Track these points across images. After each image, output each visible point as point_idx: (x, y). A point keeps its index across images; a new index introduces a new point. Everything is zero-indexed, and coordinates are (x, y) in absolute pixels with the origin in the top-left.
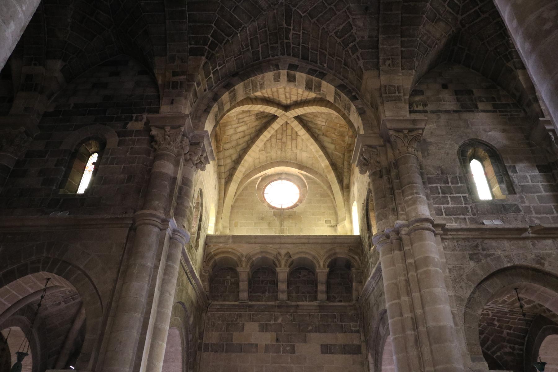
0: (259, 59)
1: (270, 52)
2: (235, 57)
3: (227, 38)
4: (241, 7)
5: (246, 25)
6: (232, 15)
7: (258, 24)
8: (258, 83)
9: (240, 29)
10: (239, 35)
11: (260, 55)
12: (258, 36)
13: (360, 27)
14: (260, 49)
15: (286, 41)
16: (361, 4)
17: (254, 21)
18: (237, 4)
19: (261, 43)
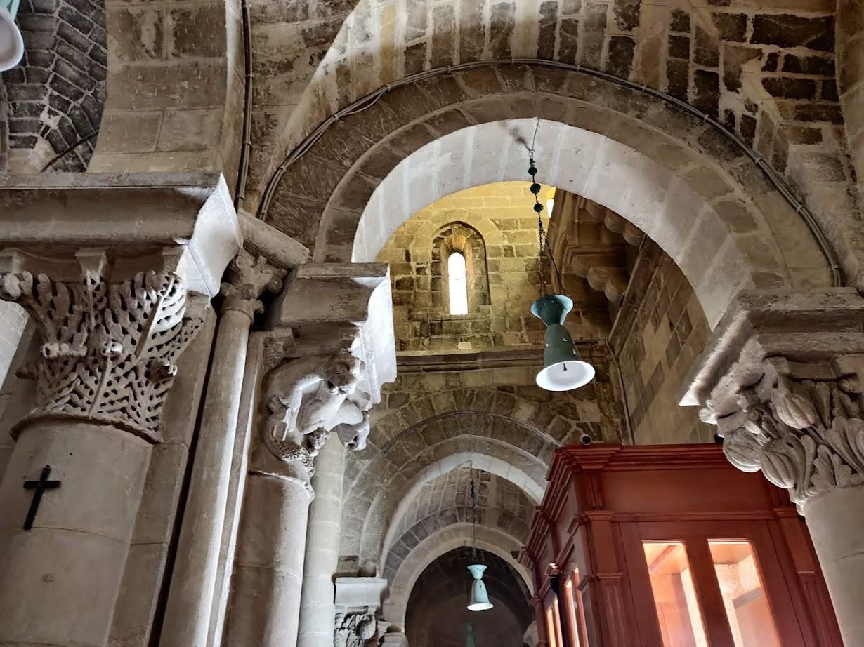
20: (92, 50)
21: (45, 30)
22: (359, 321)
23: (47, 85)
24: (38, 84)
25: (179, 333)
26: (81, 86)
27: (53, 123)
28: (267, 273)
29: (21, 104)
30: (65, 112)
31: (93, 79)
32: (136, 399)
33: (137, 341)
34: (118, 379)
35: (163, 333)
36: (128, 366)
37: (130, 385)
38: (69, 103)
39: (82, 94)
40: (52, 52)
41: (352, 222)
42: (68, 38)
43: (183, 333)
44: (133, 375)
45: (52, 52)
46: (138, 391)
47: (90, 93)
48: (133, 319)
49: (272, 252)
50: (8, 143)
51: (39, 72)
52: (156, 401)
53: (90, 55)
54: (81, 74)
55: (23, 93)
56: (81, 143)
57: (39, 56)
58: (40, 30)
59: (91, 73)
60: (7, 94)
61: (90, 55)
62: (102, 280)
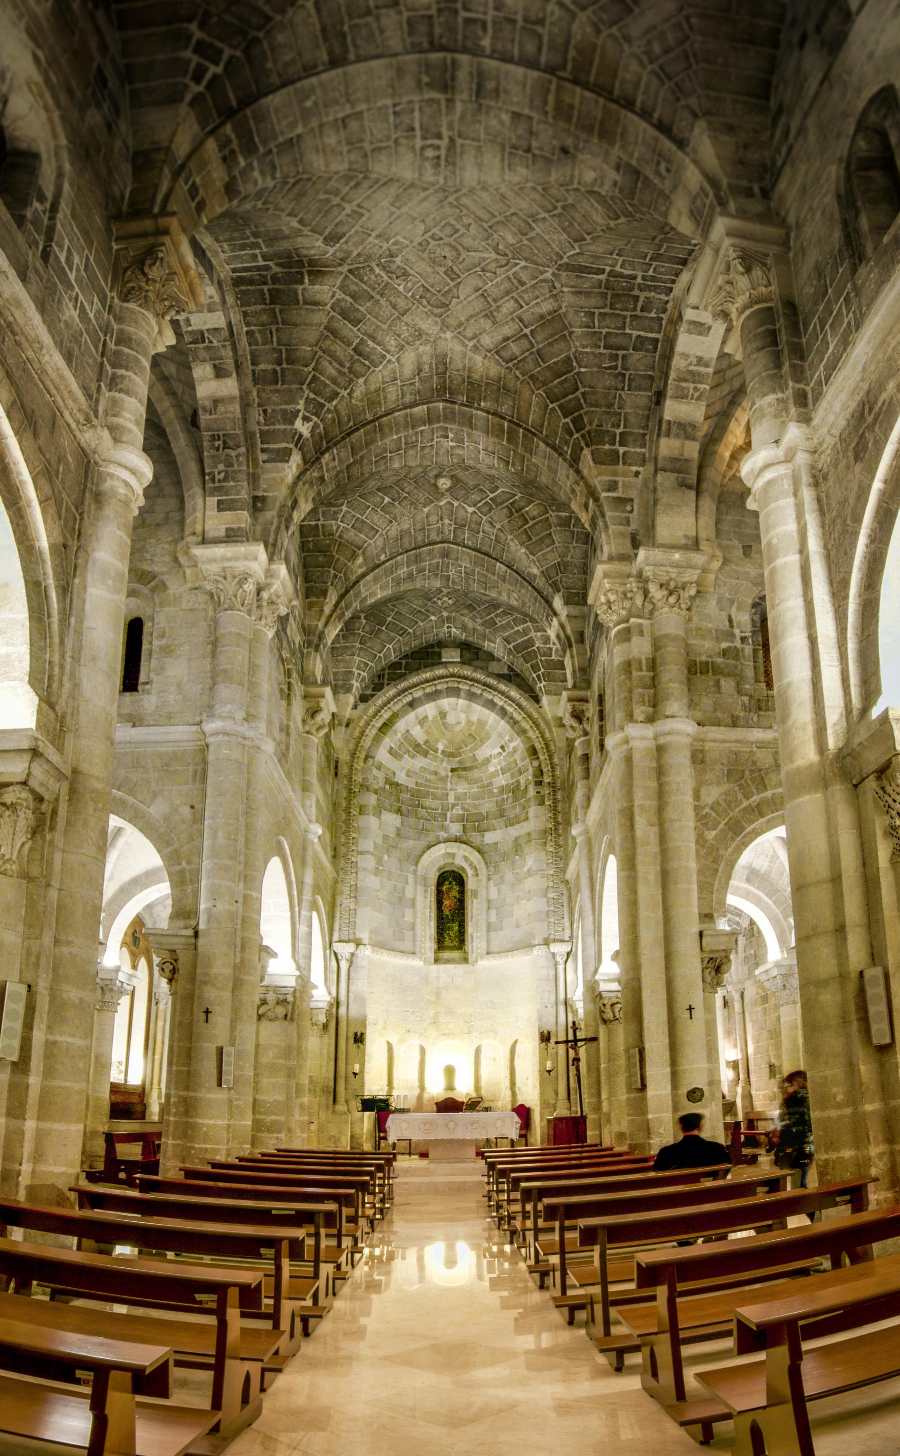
0: (657, 340)
1: (653, 315)
2: (623, 389)
3: (578, 393)
4: (541, 346)
5: (573, 350)
6: (548, 367)
7: (581, 327)
8: (695, 368)
9: (574, 364)
10: (583, 370)
11: (650, 335)
12: (604, 331)
13: (596, 180)
14: (635, 333)
15: (639, 280)
16: (555, 158)
17: (571, 333)
18: (534, 350)
19: (624, 328)
20: (358, 344)
21: (312, 325)
23: (304, 387)
24: (295, 386)
26: (338, 385)
27: (303, 428)
29: (273, 411)
30: (318, 417)
31: (351, 376)
38: (324, 406)
39: (338, 394)
40: (315, 349)
42: (334, 333)
45: (315, 349)
47: (345, 393)
50: (262, 457)
51: (296, 373)
53: (355, 350)
54: (339, 372)
55: (275, 398)
56: (328, 449)
57: (298, 354)
58: (306, 325)
59: (350, 370)
60: (257, 400)
61: (355, 350)
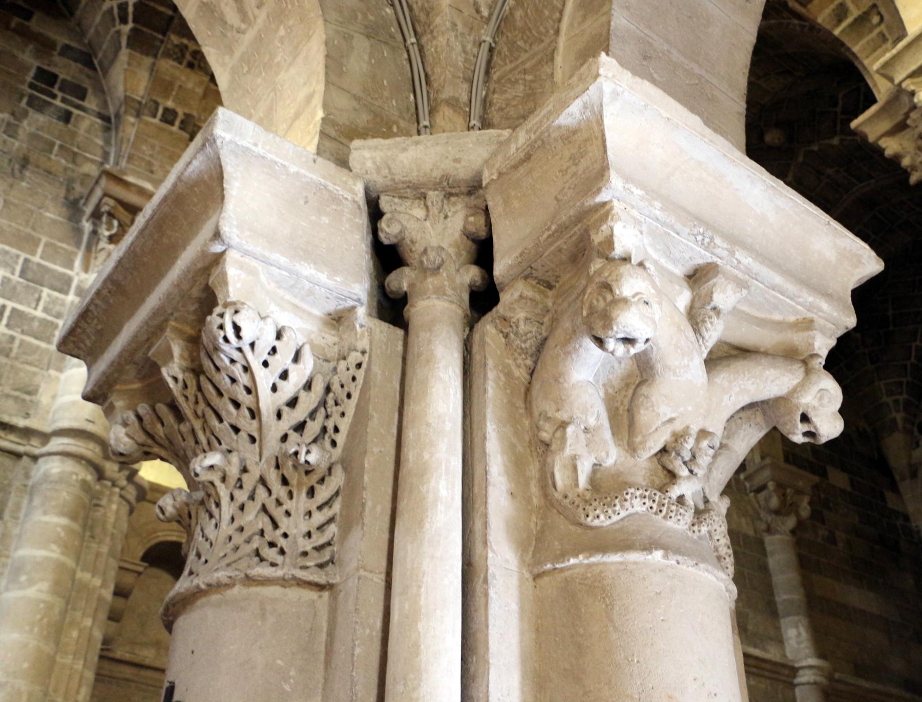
22: (599, 191)
25: (328, 389)
28: (455, 213)
32: (276, 526)
33: (256, 435)
34: (242, 508)
35: (293, 403)
36: (249, 481)
37: (264, 509)
41: (601, 35)
43: (336, 387)
44: (261, 492)
46: (278, 513)
48: (237, 405)
49: (437, 174)
52: (319, 518)
62: (184, 370)
